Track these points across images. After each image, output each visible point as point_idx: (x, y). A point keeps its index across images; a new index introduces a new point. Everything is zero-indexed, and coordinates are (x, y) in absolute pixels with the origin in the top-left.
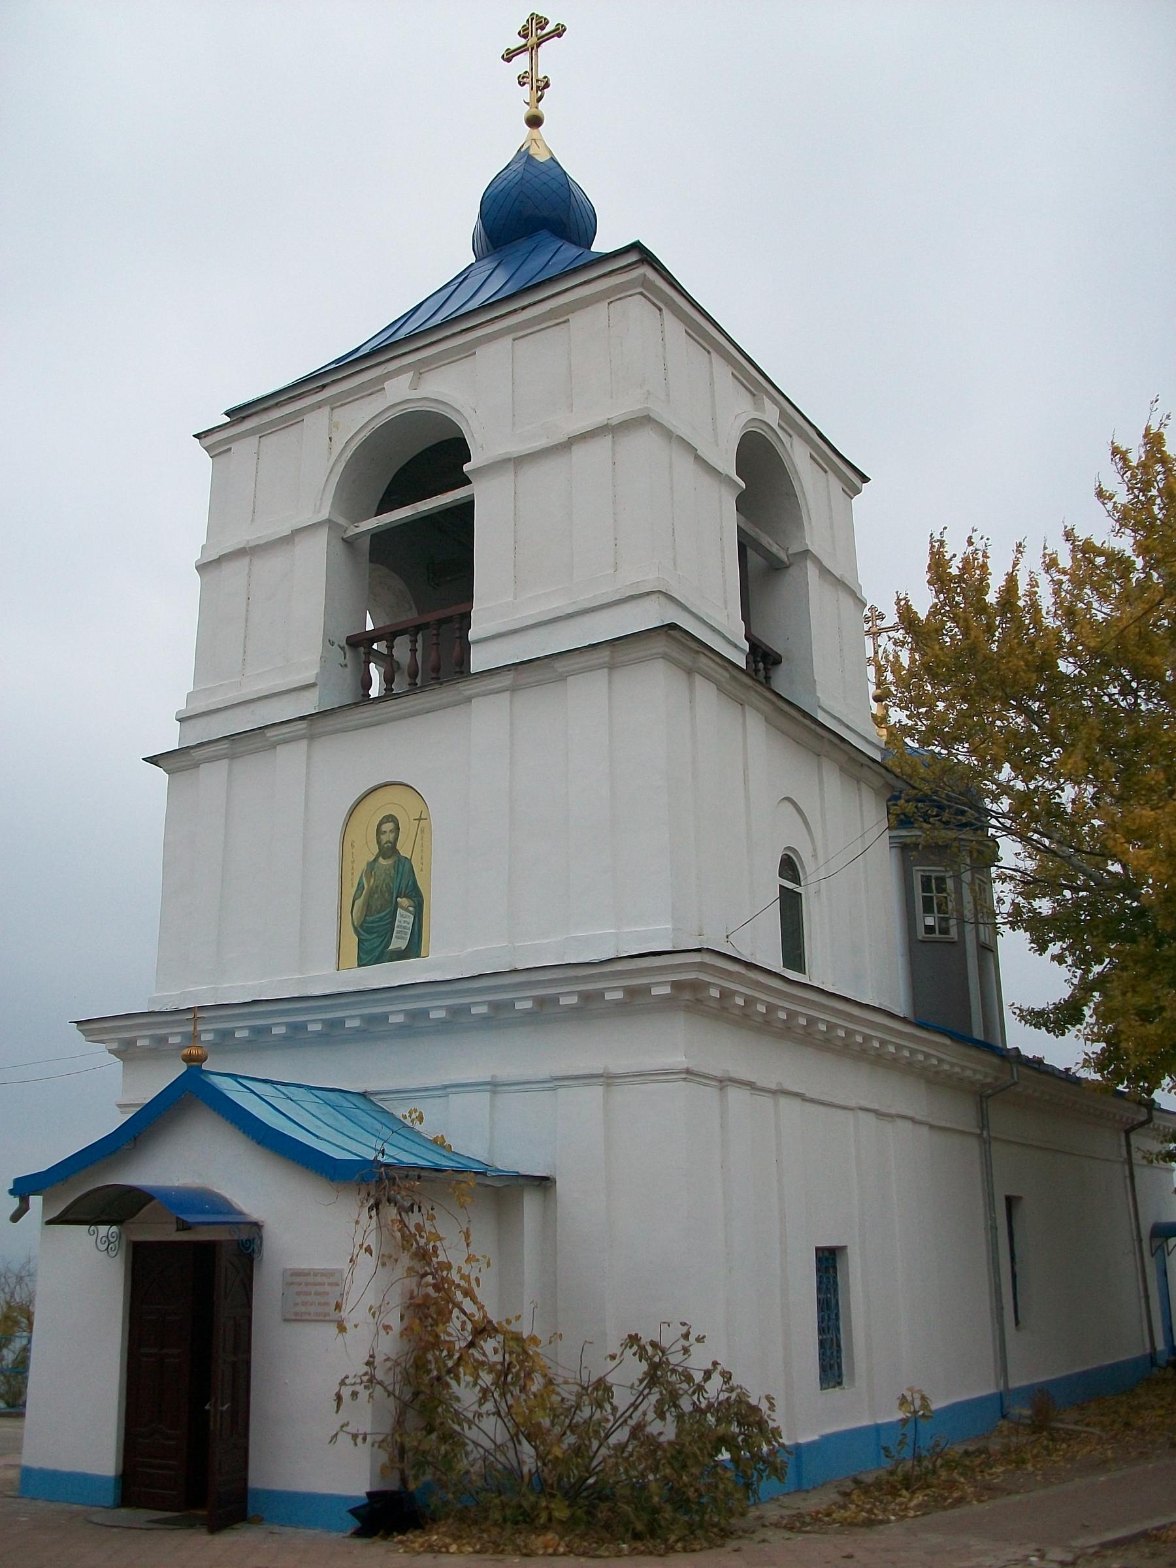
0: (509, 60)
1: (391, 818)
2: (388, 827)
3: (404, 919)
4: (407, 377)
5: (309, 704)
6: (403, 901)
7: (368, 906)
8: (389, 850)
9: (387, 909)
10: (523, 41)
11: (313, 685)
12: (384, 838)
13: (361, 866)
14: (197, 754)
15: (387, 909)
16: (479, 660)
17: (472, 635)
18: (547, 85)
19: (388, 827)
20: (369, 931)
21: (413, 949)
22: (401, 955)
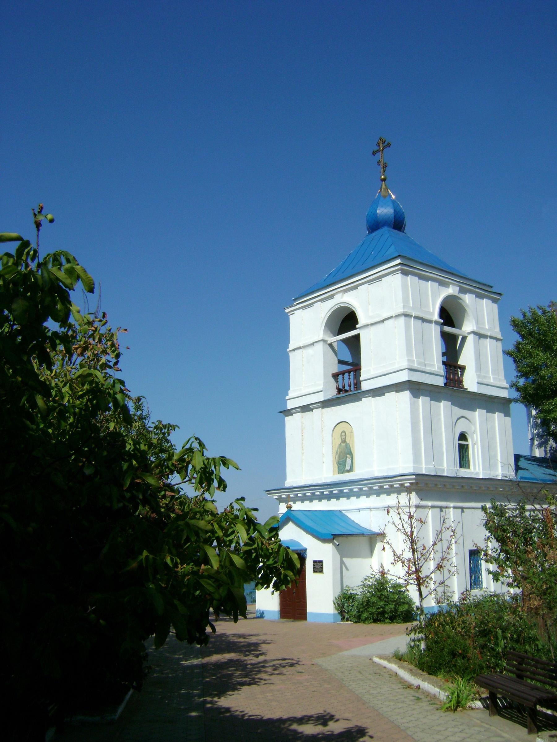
0: (374, 155)
1: (344, 432)
2: (343, 434)
3: (349, 461)
4: (340, 295)
5: (321, 397)
6: (348, 456)
7: (339, 456)
8: (344, 441)
9: (344, 457)
10: (377, 148)
11: (322, 391)
12: (343, 437)
13: (337, 445)
14: (292, 411)
15: (344, 457)
16: (365, 386)
17: (361, 379)
18: (386, 166)
19: (343, 434)
20: (340, 464)
21: (351, 470)
22: (349, 471)
